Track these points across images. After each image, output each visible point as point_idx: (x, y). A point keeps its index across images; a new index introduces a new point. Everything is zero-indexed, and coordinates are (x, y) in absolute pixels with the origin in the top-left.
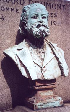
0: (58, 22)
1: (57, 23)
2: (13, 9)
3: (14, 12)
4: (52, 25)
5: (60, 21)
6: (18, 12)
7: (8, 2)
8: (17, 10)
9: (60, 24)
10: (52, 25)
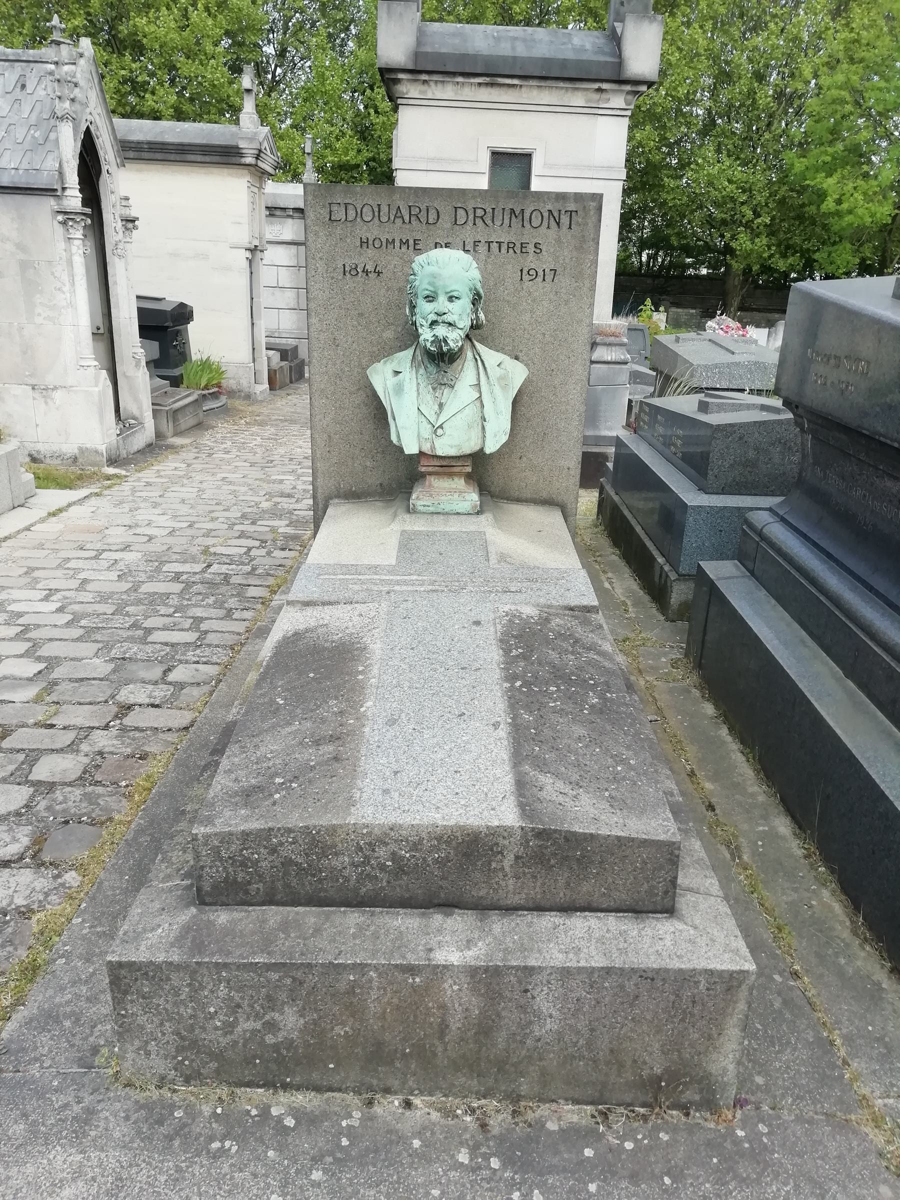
1: (541, 273)
9: (549, 278)
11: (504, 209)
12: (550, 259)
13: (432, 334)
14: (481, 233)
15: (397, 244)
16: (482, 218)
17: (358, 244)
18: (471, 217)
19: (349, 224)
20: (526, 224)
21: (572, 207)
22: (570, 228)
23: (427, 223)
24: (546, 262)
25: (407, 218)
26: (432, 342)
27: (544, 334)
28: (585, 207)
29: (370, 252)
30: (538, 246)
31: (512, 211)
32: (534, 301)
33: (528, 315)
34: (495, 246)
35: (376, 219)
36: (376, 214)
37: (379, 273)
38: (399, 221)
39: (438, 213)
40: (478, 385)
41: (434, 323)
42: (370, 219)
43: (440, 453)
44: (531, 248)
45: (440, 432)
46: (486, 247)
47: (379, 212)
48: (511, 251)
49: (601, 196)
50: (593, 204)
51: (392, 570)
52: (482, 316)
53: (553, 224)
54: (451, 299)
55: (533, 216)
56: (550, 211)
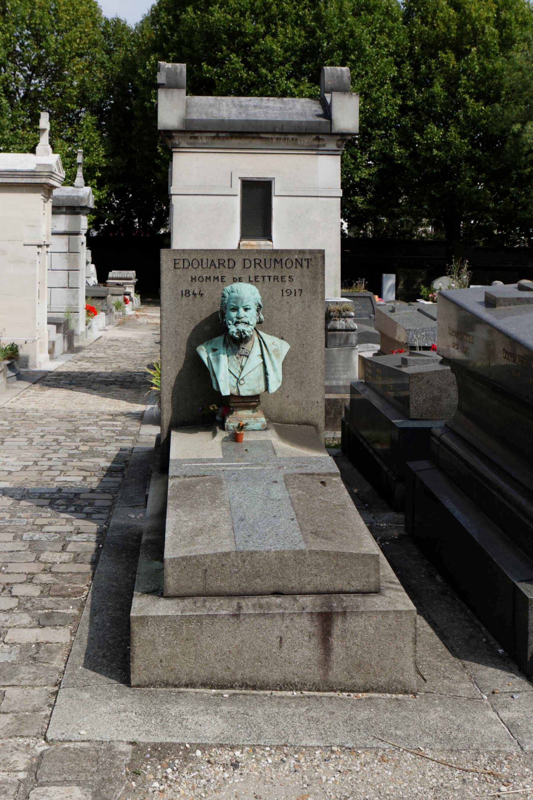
1: (293, 292)
5: (300, 288)
8: (222, 278)
9: (298, 294)
14: (260, 272)
15: (212, 279)
16: (259, 264)
17: (190, 279)
18: (253, 263)
19: (185, 270)
20: (284, 266)
21: (308, 256)
23: (229, 267)
24: (296, 286)
25: (217, 265)
26: (237, 333)
27: (297, 325)
29: (197, 282)
31: (276, 260)
32: (290, 306)
33: (287, 314)
34: (267, 279)
35: (200, 267)
37: (202, 295)
38: (213, 267)
40: (262, 356)
41: (236, 323)
43: (243, 394)
44: (287, 279)
45: (242, 382)
46: (262, 279)
48: (276, 280)
49: (324, 251)
50: (319, 255)
51: (221, 461)
52: (262, 317)
54: (246, 309)
56: (296, 260)
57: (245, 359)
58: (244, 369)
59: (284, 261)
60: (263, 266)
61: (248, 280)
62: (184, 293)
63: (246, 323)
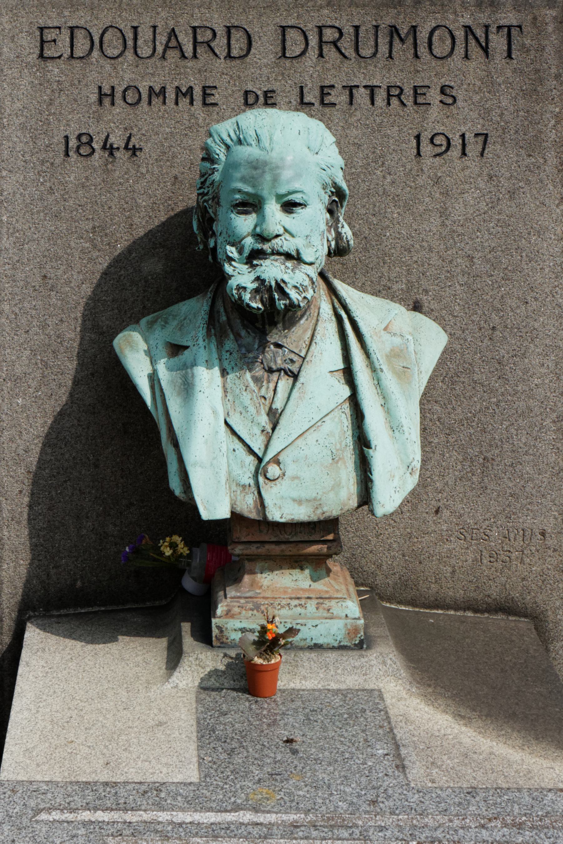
0: (463, 136)
1: (456, 141)
2: (184, 90)
3: (191, 103)
4: (419, 154)
5: (479, 129)
6: (215, 104)
7: (163, 57)
8: (206, 92)
9: (473, 149)
10: (419, 154)
11: (377, 27)
12: (474, 115)
13: (252, 276)
15: (171, 95)
16: (334, 43)
17: (94, 97)
18: (313, 41)
19: (77, 64)
20: (423, 50)
22: (509, 56)
23: (229, 56)
25: (188, 49)
27: (471, 258)
28: (535, 18)
30: (448, 91)
31: (394, 30)
32: (446, 194)
33: (436, 221)
34: (362, 95)
35: (129, 55)
36: (130, 43)
37: (134, 151)
38: (173, 54)
39: (249, 37)
42: (116, 52)
44: (434, 96)
46: (344, 98)
47: (135, 39)
48: (395, 102)
52: (346, 231)
53: (475, 51)
55: (435, 38)
56: (468, 29)
57: (284, 383)
58: (283, 422)
59: (423, 35)
60: (350, 52)
61: (295, 99)
62: (73, 143)
63: (288, 256)
